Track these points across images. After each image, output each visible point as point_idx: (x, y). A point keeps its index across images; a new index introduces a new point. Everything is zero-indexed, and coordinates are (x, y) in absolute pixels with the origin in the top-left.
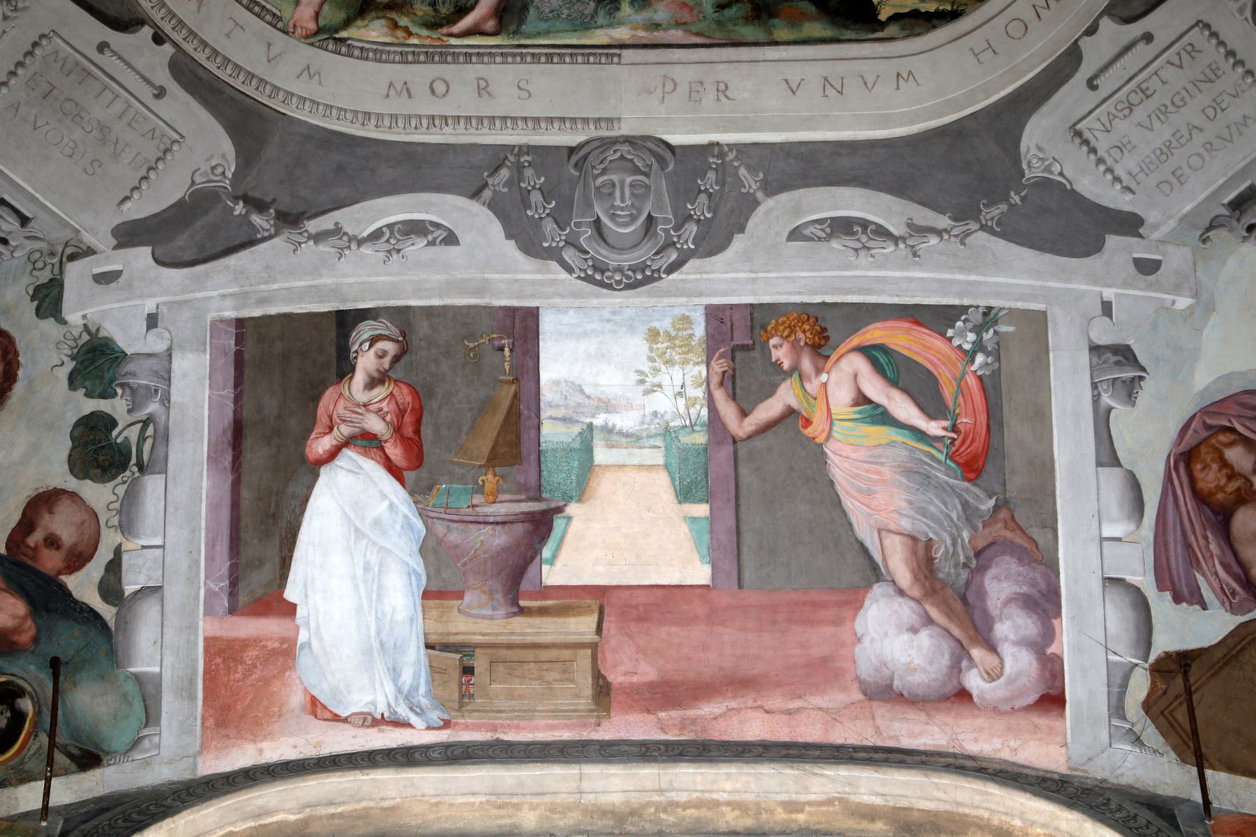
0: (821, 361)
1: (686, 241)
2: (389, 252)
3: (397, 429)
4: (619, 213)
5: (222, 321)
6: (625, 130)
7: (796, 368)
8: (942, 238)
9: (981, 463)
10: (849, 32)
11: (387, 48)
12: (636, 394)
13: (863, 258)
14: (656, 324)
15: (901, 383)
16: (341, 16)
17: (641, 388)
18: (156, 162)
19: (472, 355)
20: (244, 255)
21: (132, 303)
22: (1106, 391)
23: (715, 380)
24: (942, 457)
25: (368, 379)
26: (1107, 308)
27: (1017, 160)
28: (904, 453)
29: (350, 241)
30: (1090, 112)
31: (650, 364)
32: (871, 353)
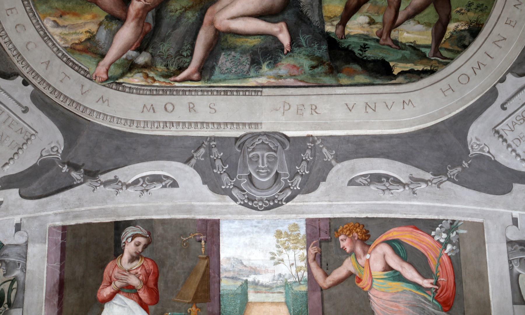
0: (366, 248)
1: (296, 186)
2: (142, 191)
3: (145, 284)
4: (261, 171)
5: (55, 227)
6: (264, 129)
7: (353, 251)
8: (428, 185)
9: (451, 302)
10: (378, 80)
11: (143, 88)
12: (270, 265)
13: (387, 195)
14: (280, 228)
15: (407, 261)
16: (120, 71)
17: (273, 261)
18: (23, 145)
19: (185, 244)
20: (67, 193)
21: (7, 218)
22: (516, 265)
23: (311, 257)
24: (430, 299)
25: (130, 257)
26: (515, 222)
27: (466, 145)
28: (411, 296)
29: (122, 185)
30: (503, 121)
31: (277, 249)
32: (391, 243)
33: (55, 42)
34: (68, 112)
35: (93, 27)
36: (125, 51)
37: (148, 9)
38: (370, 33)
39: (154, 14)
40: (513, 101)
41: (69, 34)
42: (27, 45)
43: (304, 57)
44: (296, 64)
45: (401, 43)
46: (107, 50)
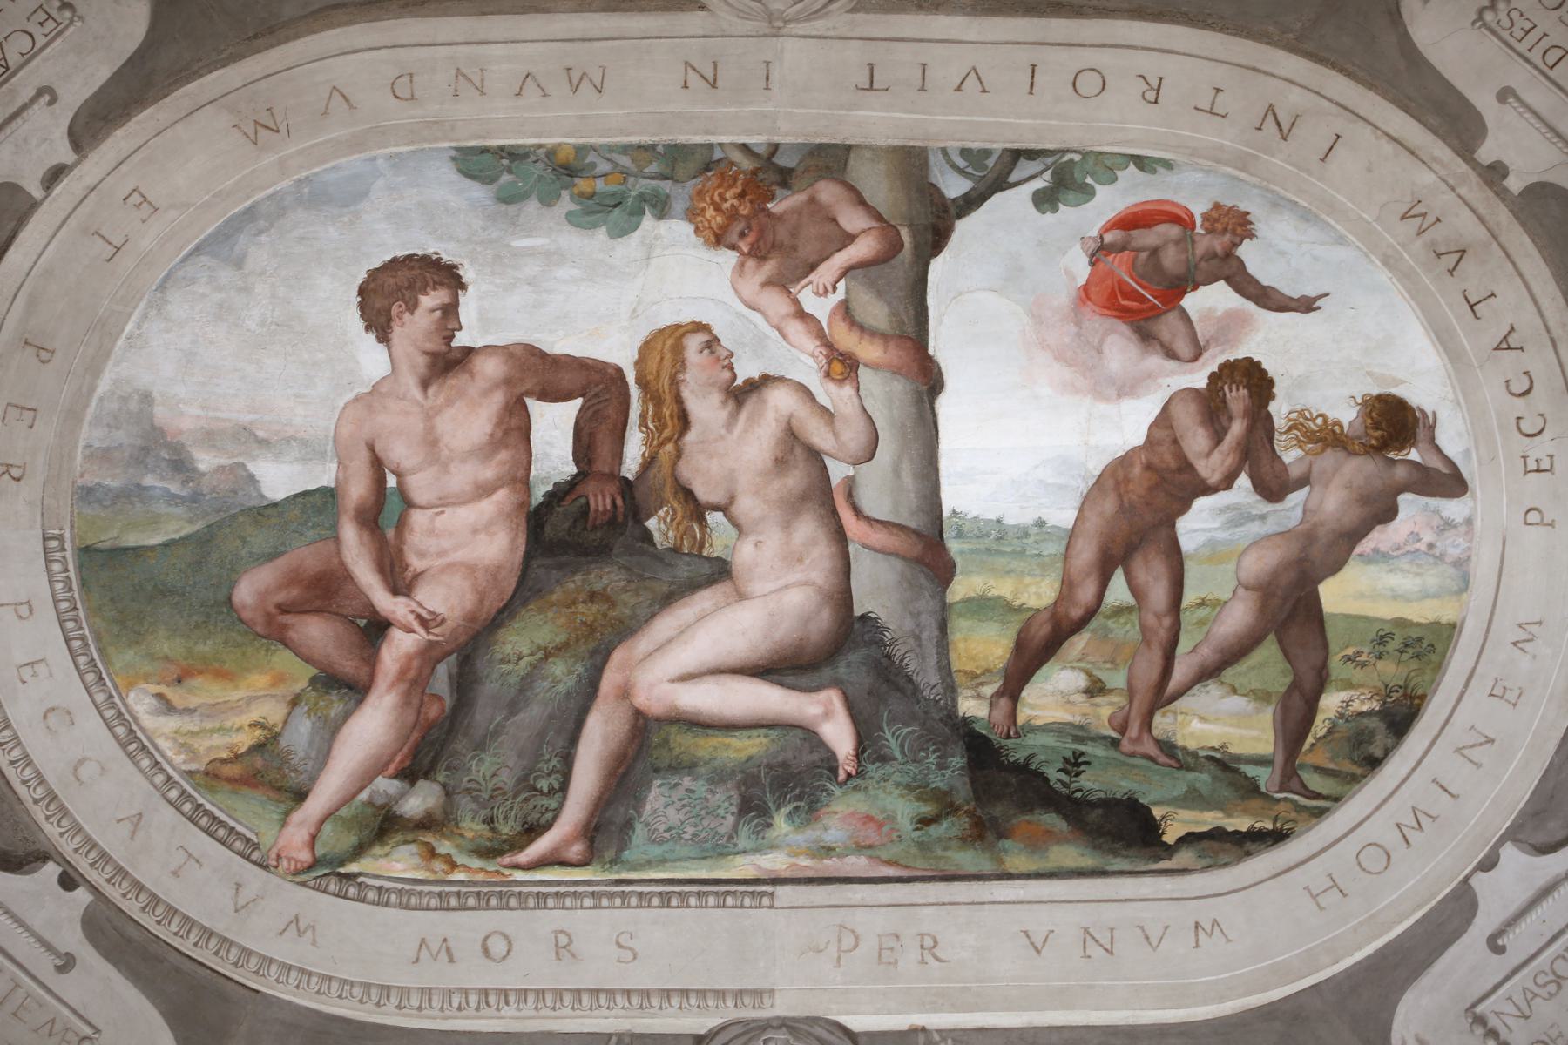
6: (781, 1007)
10: (1118, 860)
11: (419, 888)
16: (351, 840)
30: (1496, 987)
33: (159, 759)
34: (194, 966)
35: (273, 712)
36: (367, 777)
37: (436, 653)
38: (1092, 720)
39: (455, 670)
40: (1524, 926)
41: (202, 732)
42: (76, 769)
43: (897, 792)
44: (874, 813)
45: (1184, 749)
46: (314, 779)
